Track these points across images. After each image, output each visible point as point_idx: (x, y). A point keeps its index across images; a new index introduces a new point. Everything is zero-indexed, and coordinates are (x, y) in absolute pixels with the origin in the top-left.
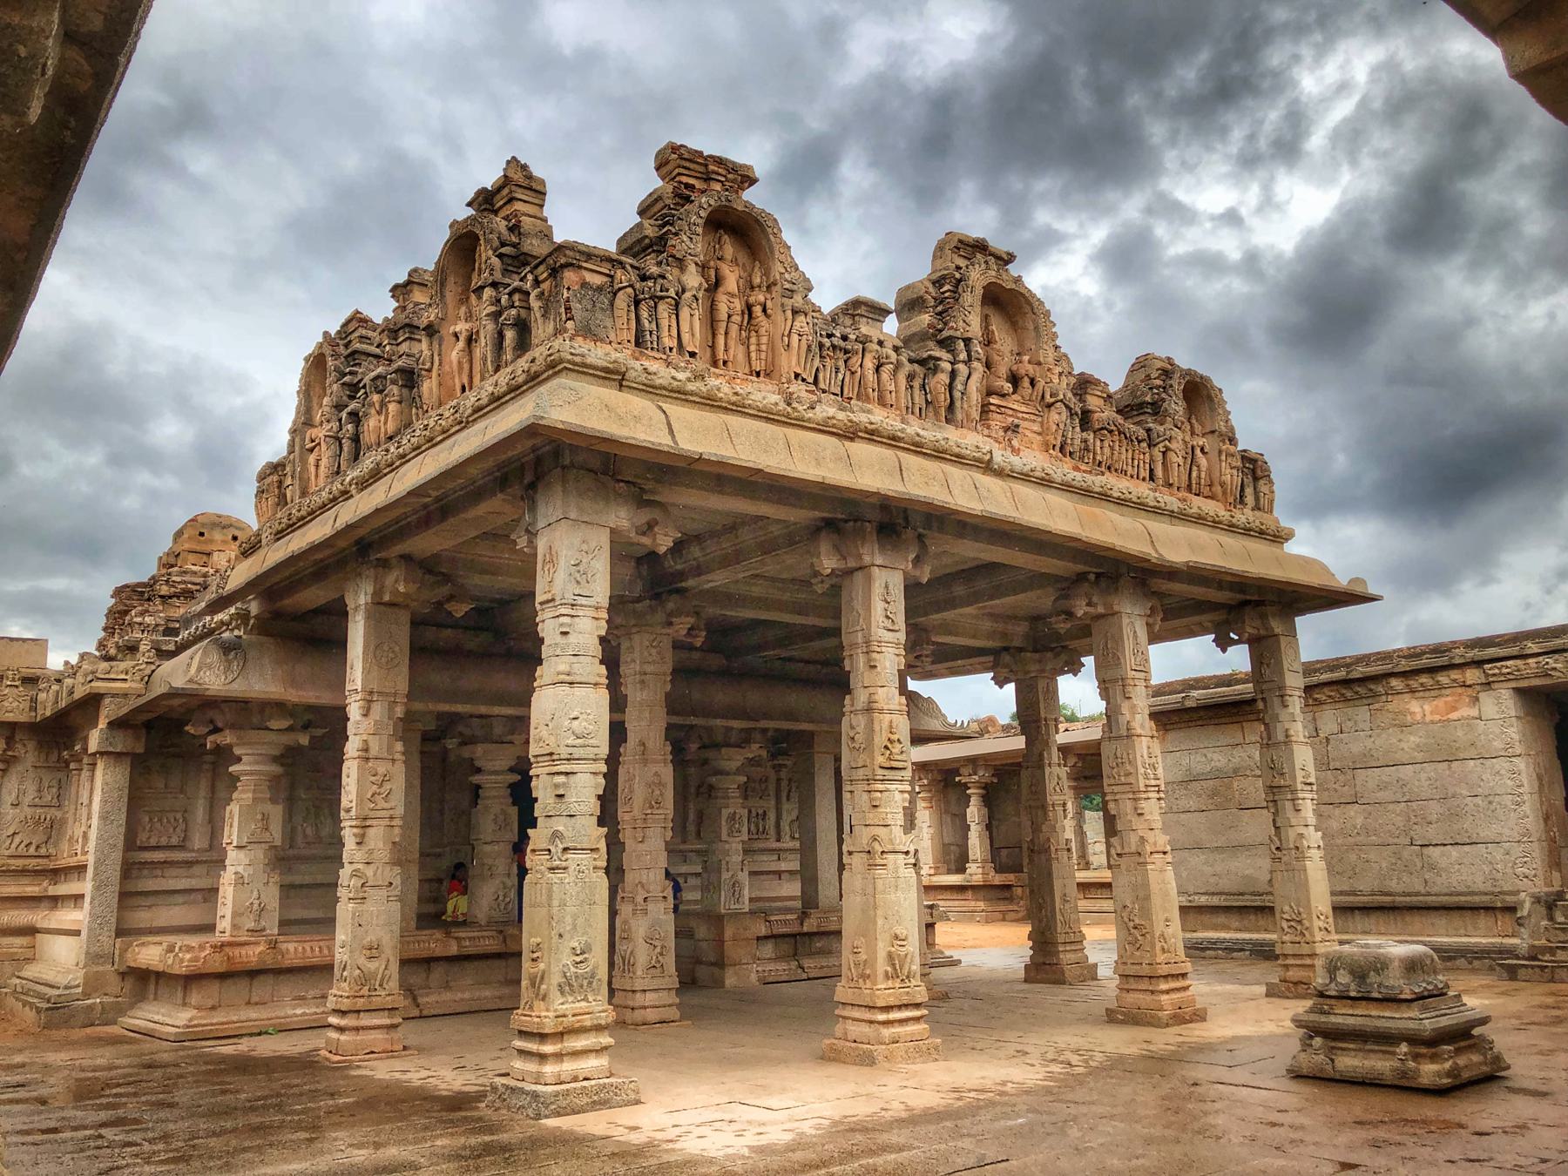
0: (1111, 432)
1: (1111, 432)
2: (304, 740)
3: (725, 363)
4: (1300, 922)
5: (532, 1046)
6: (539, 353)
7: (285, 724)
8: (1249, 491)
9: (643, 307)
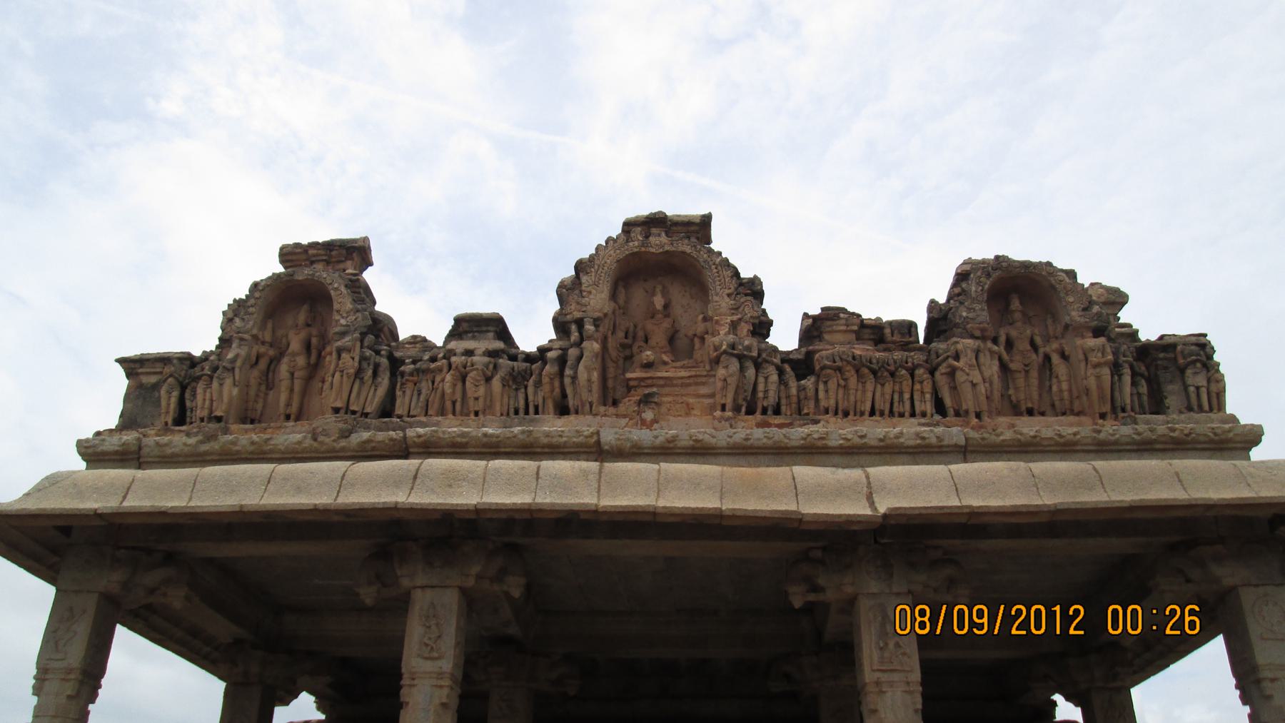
0: (839, 369)
1: (839, 369)
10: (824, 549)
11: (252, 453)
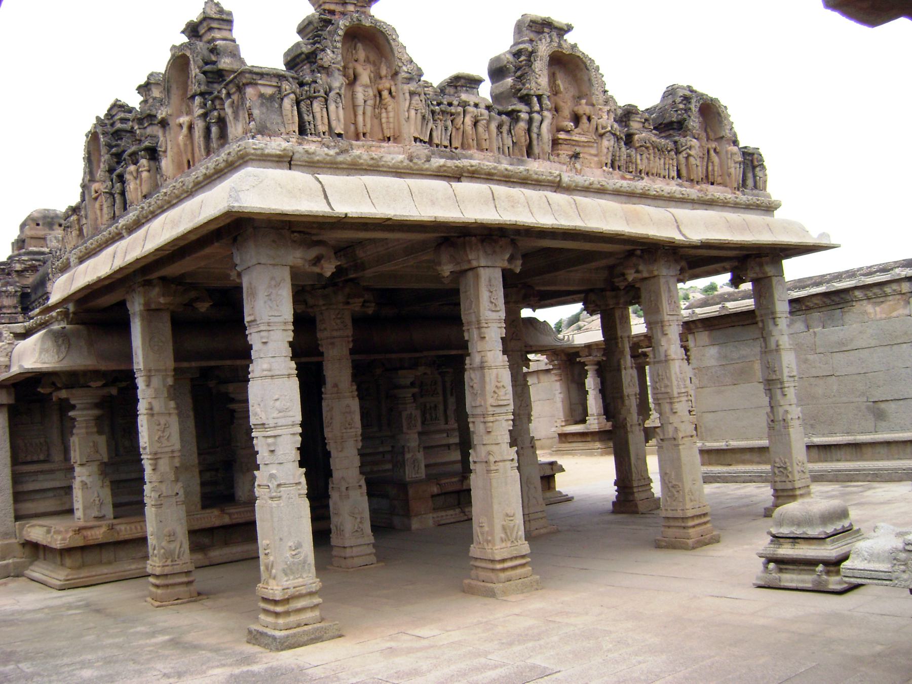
0: (647, 148)
1: (647, 148)
2: (114, 391)
3: (364, 134)
4: (785, 468)
5: (271, 607)
6: (233, 148)
7: (100, 384)
8: (750, 175)
9: (302, 104)
11: (370, 166)
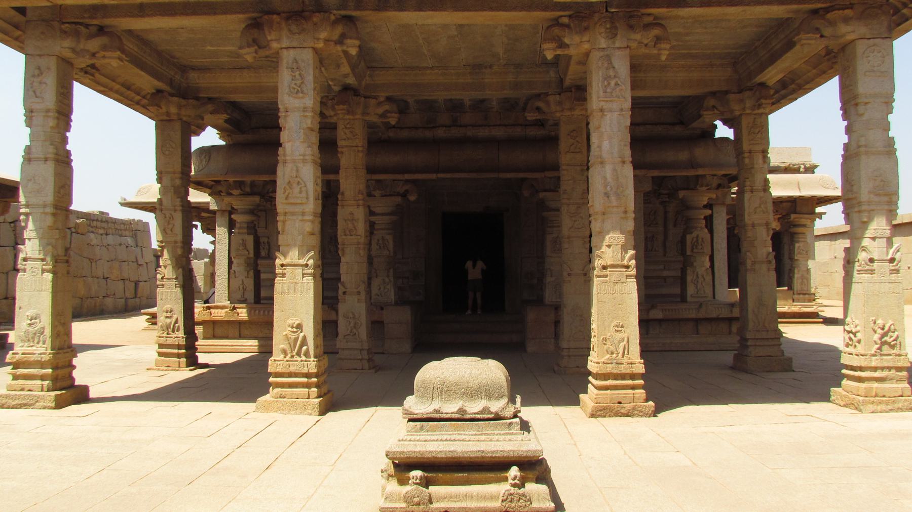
10: (570, 16)
